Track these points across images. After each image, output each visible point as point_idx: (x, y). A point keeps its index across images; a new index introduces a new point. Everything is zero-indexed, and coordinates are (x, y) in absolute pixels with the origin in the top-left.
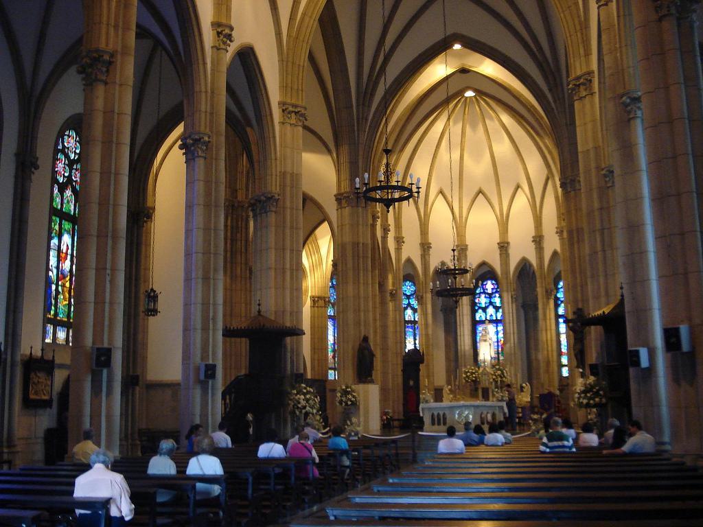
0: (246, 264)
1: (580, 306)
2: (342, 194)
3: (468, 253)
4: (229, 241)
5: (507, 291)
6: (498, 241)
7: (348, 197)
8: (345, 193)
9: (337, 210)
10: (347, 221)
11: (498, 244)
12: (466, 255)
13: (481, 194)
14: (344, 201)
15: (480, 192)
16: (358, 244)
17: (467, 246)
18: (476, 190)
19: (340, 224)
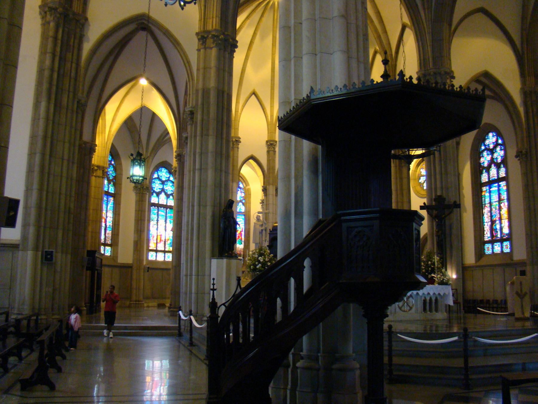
0: (75, 94)
1: (439, 193)
2: (209, 32)
3: (239, 146)
4: (57, 59)
5: (273, 185)
6: (267, 140)
7: (217, 36)
8: (216, 30)
9: (199, 50)
10: (213, 63)
11: (267, 142)
12: (238, 148)
13: (253, 96)
14: (210, 42)
15: (254, 93)
16: (223, 92)
17: (240, 138)
18: (250, 91)
19: (202, 66)
